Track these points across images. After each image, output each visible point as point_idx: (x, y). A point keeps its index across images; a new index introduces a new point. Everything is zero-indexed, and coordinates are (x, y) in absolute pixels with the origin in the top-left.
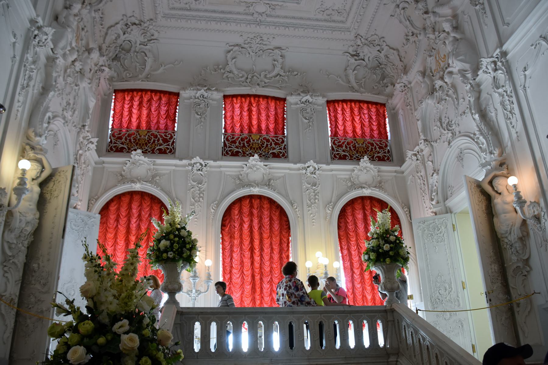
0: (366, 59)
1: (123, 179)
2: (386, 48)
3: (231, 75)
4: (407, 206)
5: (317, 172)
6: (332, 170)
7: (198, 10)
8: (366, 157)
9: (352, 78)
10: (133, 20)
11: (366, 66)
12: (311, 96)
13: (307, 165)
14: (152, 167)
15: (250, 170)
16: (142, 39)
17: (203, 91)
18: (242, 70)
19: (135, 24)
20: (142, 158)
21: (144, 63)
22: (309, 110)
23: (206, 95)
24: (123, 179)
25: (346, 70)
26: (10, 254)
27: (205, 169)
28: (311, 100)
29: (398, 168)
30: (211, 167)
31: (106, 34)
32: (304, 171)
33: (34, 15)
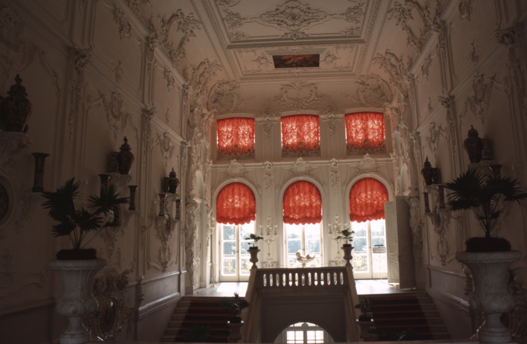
0: (370, 84)
1: (228, 175)
2: (381, 81)
3: (285, 103)
4: (392, 182)
5: (338, 165)
6: (347, 162)
7: (261, 74)
8: (367, 154)
9: (361, 98)
10: (223, 81)
11: (371, 89)
12: (334, 114)
13: (331, 161)
14: (242, 168)
15: (298, 166)
16: (230, 88)
17: (268, 117)
18: (291, 99)
19: (224, 83)
20: (237, 163)
21: (232, 102)
22: (333, 123)
23: (270, 119)
24: (228, 175)
25: (357, 92)
26: (187, 245)
27: (272, 167)
28: (334, 116)
29: (388, 159)
30: (275, 165)
31: (210, 93)
32: (330, 164)
33: (182, 140)
